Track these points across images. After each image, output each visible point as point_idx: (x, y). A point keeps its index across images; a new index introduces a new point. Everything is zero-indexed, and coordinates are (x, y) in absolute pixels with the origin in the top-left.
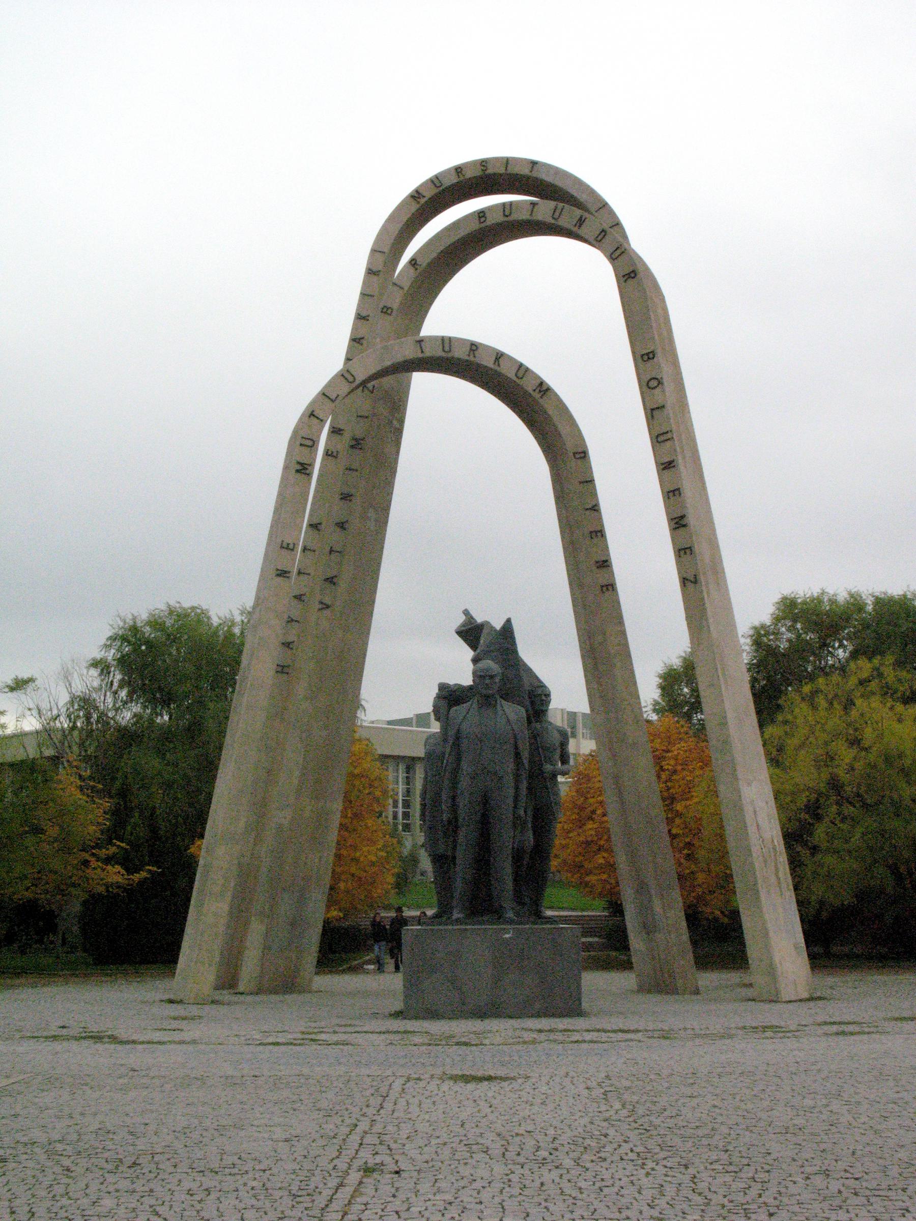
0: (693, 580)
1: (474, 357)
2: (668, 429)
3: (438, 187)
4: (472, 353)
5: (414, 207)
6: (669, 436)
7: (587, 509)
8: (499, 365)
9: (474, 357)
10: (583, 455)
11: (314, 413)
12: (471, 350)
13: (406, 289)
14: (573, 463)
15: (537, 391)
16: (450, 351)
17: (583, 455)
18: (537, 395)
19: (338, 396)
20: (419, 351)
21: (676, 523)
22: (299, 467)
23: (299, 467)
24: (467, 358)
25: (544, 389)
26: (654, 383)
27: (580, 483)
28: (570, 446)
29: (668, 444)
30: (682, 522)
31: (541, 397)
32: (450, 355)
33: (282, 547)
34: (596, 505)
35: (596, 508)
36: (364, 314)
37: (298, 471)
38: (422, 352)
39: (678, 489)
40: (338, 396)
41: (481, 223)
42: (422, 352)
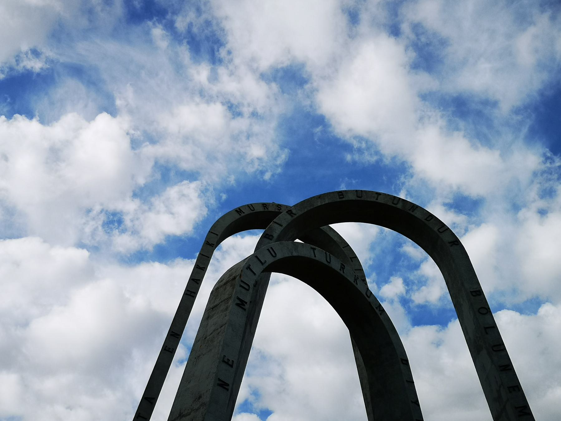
5: (237, 216)
13: (284, 225)
16: (329, 263)
18: (377, 311)
22: (239, 302)
23: (239, 302)
24: (339, 271)
26: (485, 311)
32: (330, 265)
33: (224, 361)
36: (201, 266)
37: (238, 305)
41: (340, 198)
42: (315, 256)
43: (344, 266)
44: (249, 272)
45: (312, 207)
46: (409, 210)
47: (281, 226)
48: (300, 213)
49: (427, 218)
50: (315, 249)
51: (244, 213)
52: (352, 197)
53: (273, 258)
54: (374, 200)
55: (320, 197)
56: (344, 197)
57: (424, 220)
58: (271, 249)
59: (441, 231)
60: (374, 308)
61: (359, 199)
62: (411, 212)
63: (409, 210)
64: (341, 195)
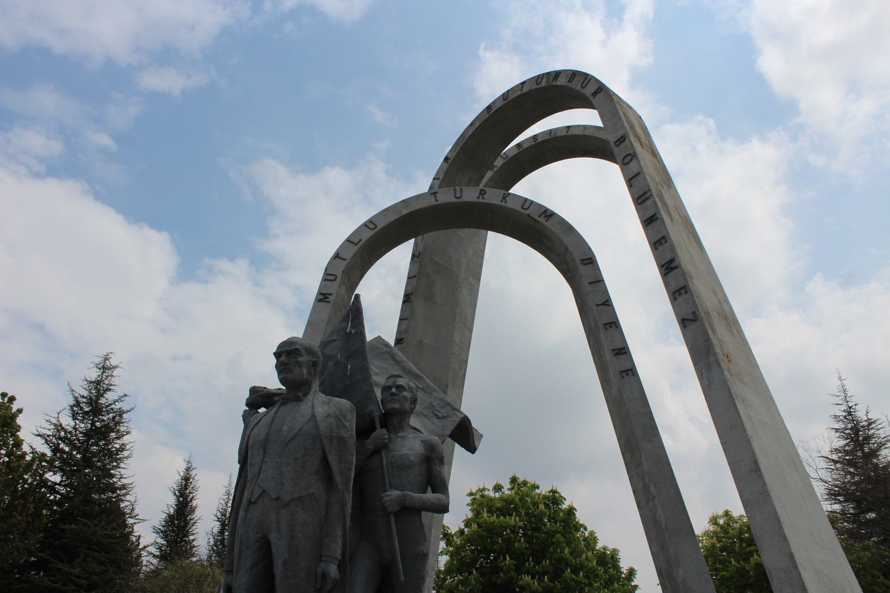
0: (692, 317)
1: (484, 199)
2: (647, 189)
3: (505, 159)
4: (481, 196)
6: (648, 195)
7: (598, 305)
8: (506, 202)
9: (484, 199)
10: (590, 260)
11: (340, 256)
12: (480, 194)
13: (441, 178)
14: (583, 269)
15: (543, 216)
17: (589, 261)
18: (542, 220)
19: (361, 240)
20: (435, 200)
21: (666, 269)
24: (476, 200)
25: (548, 214)
26: (629, 158)
27: (590, 283)
28: (577, 256)
29: (649, 202)
30: (673, 265)
31: (547, 221)
32: (461, 200)
34: (607, 301)
35: (607, 303)
38: (437, 201)
39: (663, 237)
40: (361, 240)
42: (437, 201)
43: (484, 190)
44: (338, 260)
45: (464, 141)
46: (553, 81)
47: (439, 179)
48: (455, 154)
49: (570, 79)
50: (436, 193)
51: (496, 166)
52: (499, 105)
53: (371, 231)
54: (520, 93)
55: (472, 125)
56: (491, 110)
57: (567, 84)
58: (371, 224)
59: (583, 85)
60: (536, 217)
61: (505, 102)
62: (555, 83)
63: (553, 81)
64: (488, 110)
